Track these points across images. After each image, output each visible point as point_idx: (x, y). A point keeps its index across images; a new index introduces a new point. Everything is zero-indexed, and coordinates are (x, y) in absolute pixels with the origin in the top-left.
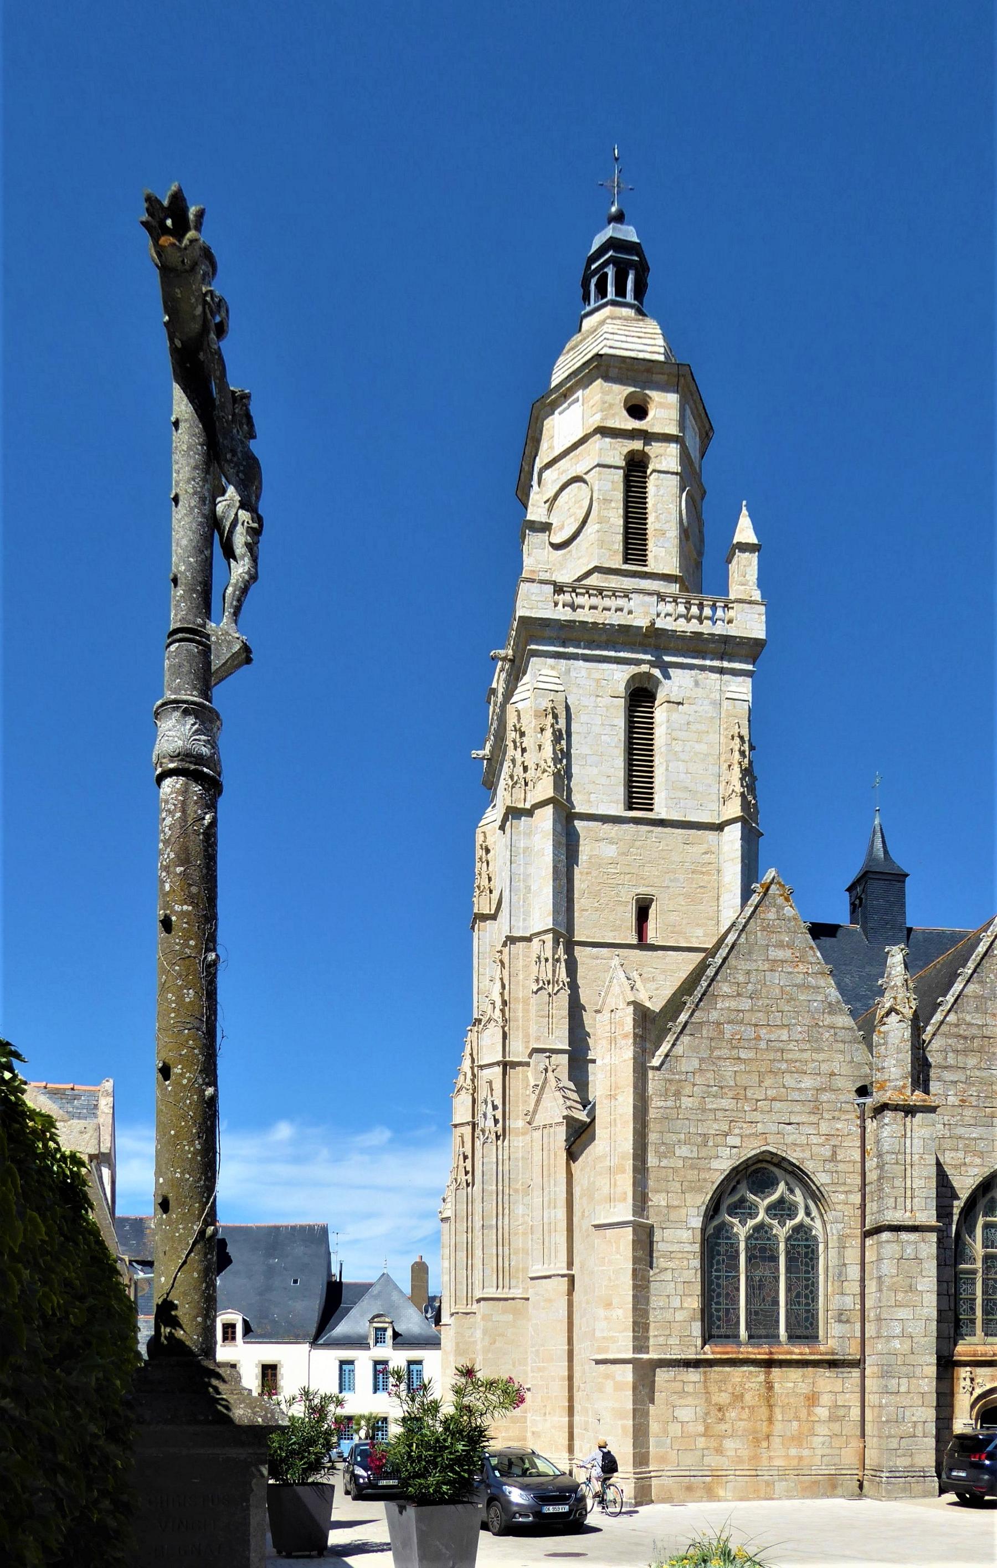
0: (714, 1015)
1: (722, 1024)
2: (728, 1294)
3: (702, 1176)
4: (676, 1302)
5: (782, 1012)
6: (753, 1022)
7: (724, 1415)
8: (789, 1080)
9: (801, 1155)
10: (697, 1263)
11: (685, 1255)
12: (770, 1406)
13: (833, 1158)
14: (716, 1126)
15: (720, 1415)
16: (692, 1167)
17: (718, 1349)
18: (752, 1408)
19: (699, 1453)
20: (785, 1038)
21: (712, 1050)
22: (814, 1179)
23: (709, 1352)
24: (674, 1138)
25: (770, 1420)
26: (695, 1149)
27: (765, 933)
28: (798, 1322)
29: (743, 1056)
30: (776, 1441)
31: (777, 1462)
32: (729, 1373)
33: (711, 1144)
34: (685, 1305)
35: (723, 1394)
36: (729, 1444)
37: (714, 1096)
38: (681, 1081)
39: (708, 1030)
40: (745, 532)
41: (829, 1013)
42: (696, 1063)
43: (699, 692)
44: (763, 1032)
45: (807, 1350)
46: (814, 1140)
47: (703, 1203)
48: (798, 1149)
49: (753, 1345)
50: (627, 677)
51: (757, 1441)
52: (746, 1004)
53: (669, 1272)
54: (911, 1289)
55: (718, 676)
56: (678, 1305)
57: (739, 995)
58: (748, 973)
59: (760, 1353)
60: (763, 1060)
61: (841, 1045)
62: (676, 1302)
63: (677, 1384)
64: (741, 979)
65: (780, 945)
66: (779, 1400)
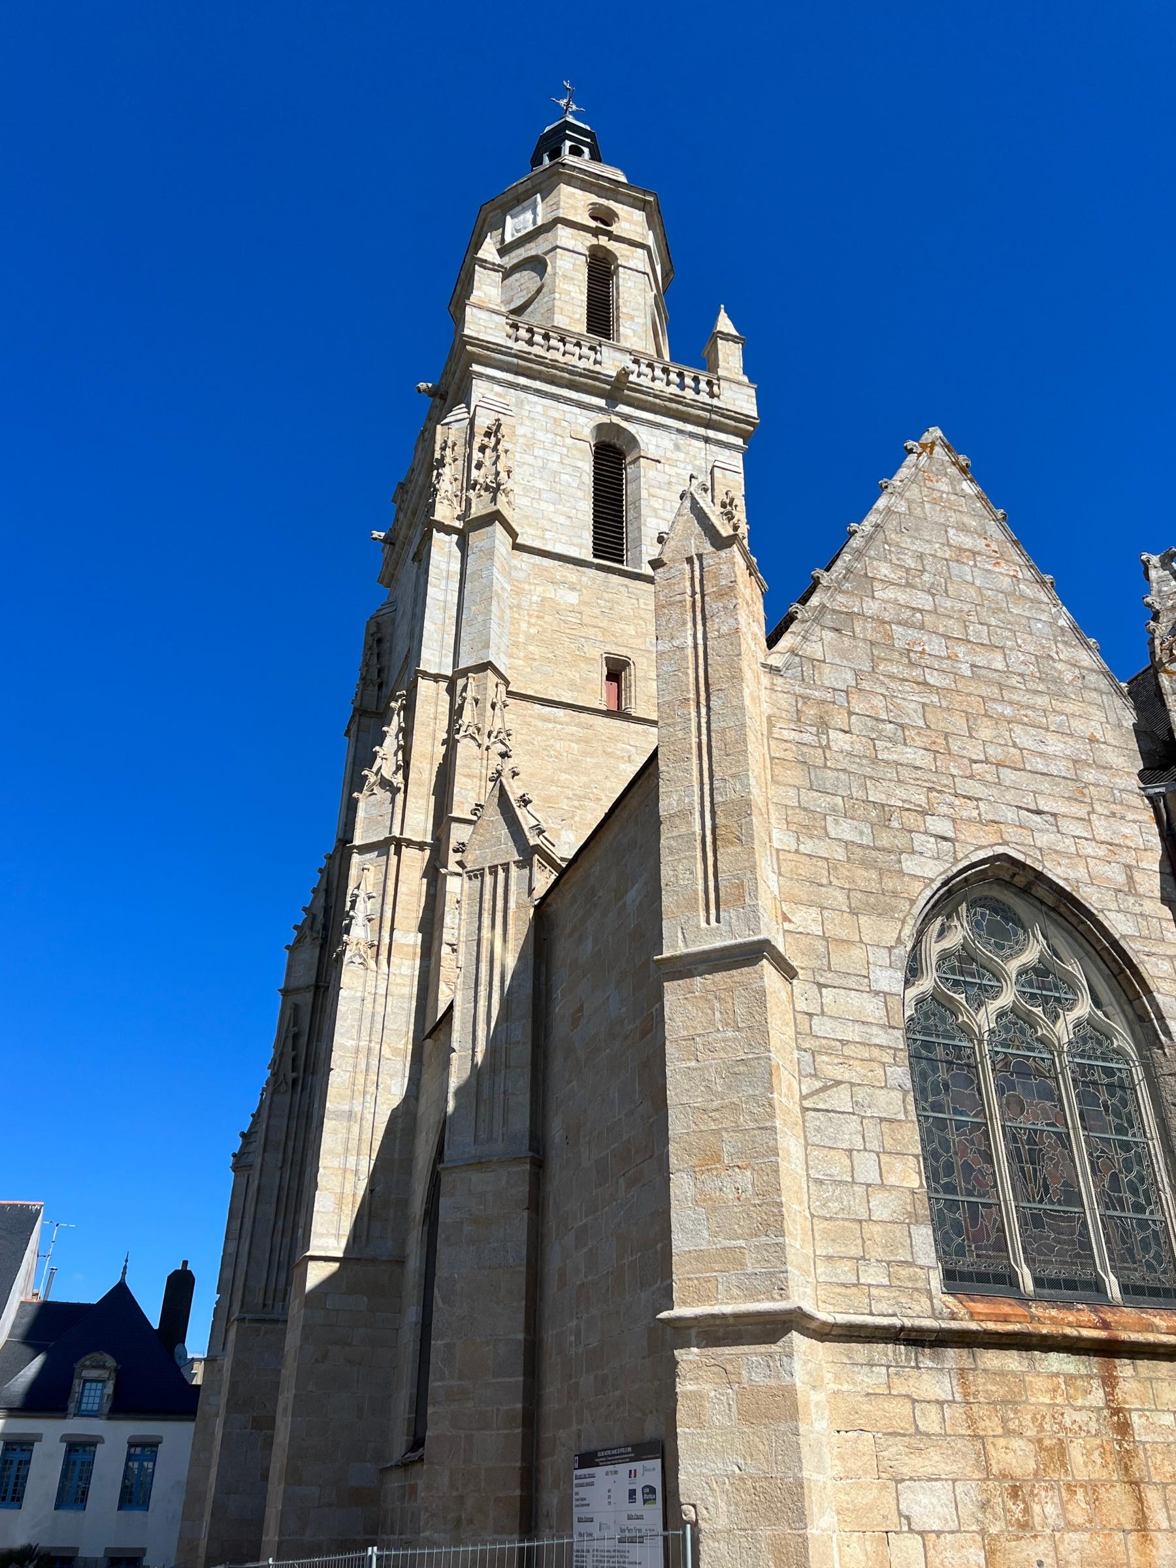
1: (886, 622)
2: (967, 1168)
3: (890, 884)
4: (867, 1169)
5: (989, 626)
6: (941, 630)
7: (1027, 1511)
8: (1023, 737)
9: (1072, 875)
10: (901, 1074)
11: (876, 1052)
12: (1135, 1484)
14: (901, 793)
15: (1017, 1510)
16: (865, 864)
17: (980, 1307)
18: (1092, 1487)
20: (999, 664)
21: (874, 662)
22: (1106, 923)
24: (824, 802)
25: (1142, 1525)
26: (867, 830)
27: (938, 508)
28: (1130, 1251)
29: (931, 681)
32: (1020, 1377)
33: (895, 824)
34: (891, 1180)
35: (1016, 1443)
37: (890, 740)
38: (824, 702)
39: (864, 629)
41: (1065, 643)
42: (849, 676)
43: (681, 456)
46: (1089, 849)
47: (899, 939)
48: (1064, 861)
49: (1052, 1302)
50: (593, 424)
52: (923, 601)
55: (702, 444)
56: (873, 1177)
57: (908, 585)
58: (921, 557)
59: (1079, 1322)
60: (969, 694)
61: (1094, 695)
62: (867, 1169)
64: (910, 562)
65: (962, 528)
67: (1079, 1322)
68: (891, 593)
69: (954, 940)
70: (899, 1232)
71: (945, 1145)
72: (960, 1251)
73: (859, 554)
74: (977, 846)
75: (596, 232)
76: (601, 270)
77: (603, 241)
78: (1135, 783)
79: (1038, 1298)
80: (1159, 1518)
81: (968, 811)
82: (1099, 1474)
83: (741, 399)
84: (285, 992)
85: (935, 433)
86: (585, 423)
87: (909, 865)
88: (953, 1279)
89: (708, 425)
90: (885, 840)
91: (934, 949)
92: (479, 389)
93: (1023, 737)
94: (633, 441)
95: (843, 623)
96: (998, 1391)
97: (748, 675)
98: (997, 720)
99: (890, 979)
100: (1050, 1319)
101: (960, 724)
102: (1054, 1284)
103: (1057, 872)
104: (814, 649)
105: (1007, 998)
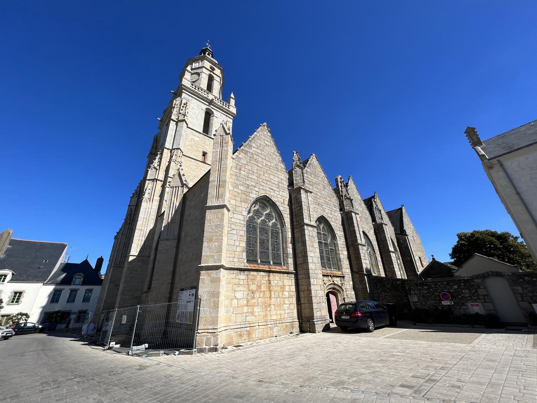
2: (253, 244)
3: (247, 198)
4: (237, 243)
8: (272, 177)
10: (245, 229)
16: (244, 194)
17: (252, 265)
18: (264, 292)
19: (244, 315)
23: (249, 266)
24: (239, 183)
25: (270, 297)
30: (273, 307)
31: (274, 317)
36: (256, 309)
40: (232, 96)
42: (246, 162)
45: (280, 268)
46: (279, 196)
49: (263, 265)
51: (266, 307)
53: (235, 231)
54: (313, 246)
59: (266, 268)
62: (237, 243)
63: (236, 280)
65: (267, 141)
66: (274, 288)
67: (266, 268)
68: (254, 149)
69: (256, 208)
70: (241, 253)
71: (250, 240)
72: (250, 257)
73: (250, 141)
74: (262, 193)
75: (211, 71)
76: (211, 79)
77: (212, 73)
78: (287, 187)
79: (260, 264)
80: (273, 296)
81: (262, 187)
82: (265, 289)
83: (233, 110)
84: (129, 206)
85: (265, 124)
86: (204, 107)
87: (251, 195)
88: (248, 261)
89: (227, 113)
90: (248, 190)
91: (253, 209)
92: (184, 95)
93: (272, 177)
94: (213, 113)
95: (246, 153)
96: (252, 278)
97: (229, 158)
98: (268, 173)
99: (245, 213)
100: (262, 267)
101: (262, 173)
102: (263, 262)
103: (274, 199)
104: (240, 156)
105: (263, 218)
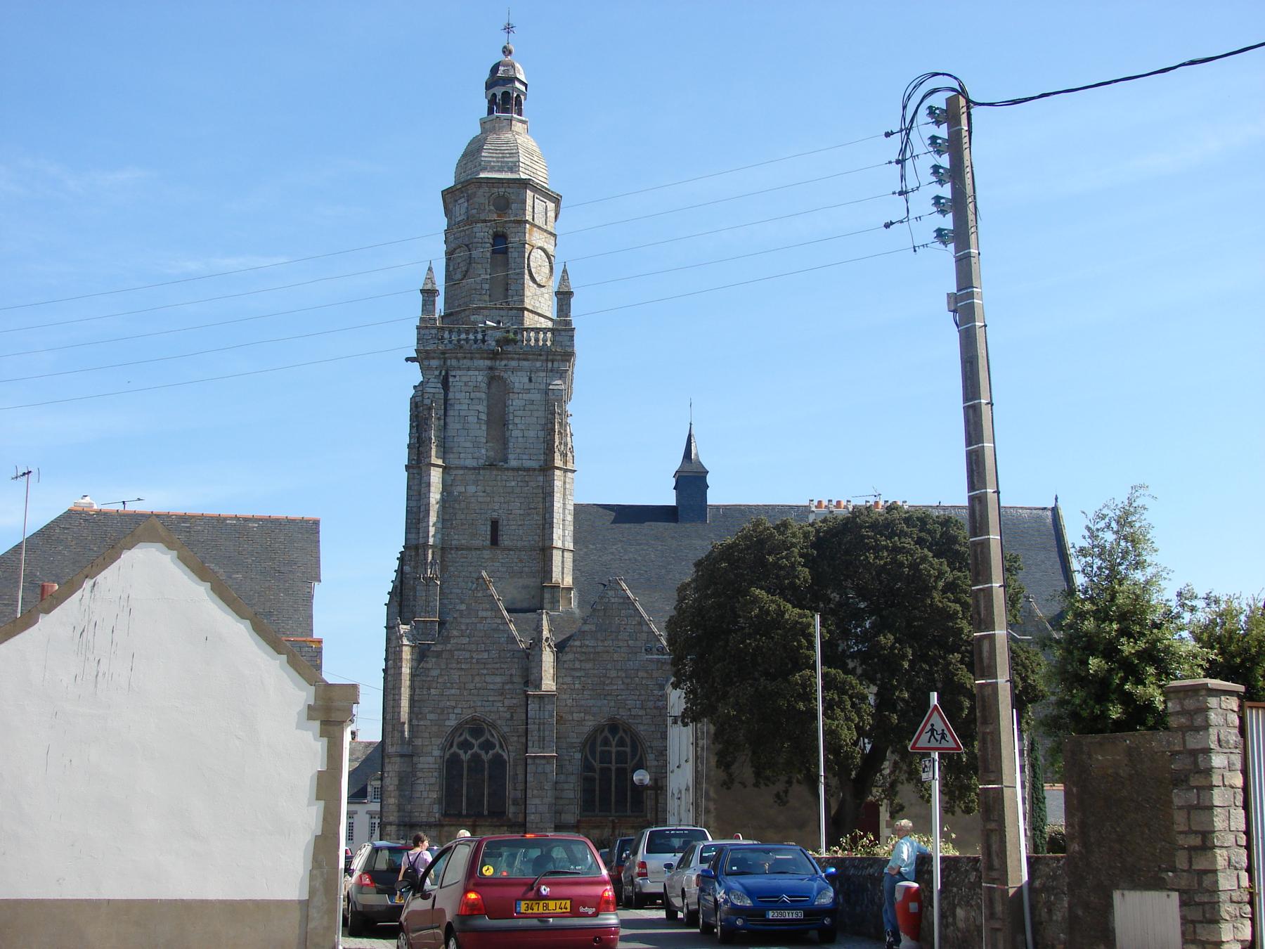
0: (449, 647)
8: (488, 679)
13: (512, 718)
44: (474, 655)
54: (542, 789)
62: (425, 795)
69: (462, 738)
74: (468, 714)
99: (437, 753)
104: (429, 666)
